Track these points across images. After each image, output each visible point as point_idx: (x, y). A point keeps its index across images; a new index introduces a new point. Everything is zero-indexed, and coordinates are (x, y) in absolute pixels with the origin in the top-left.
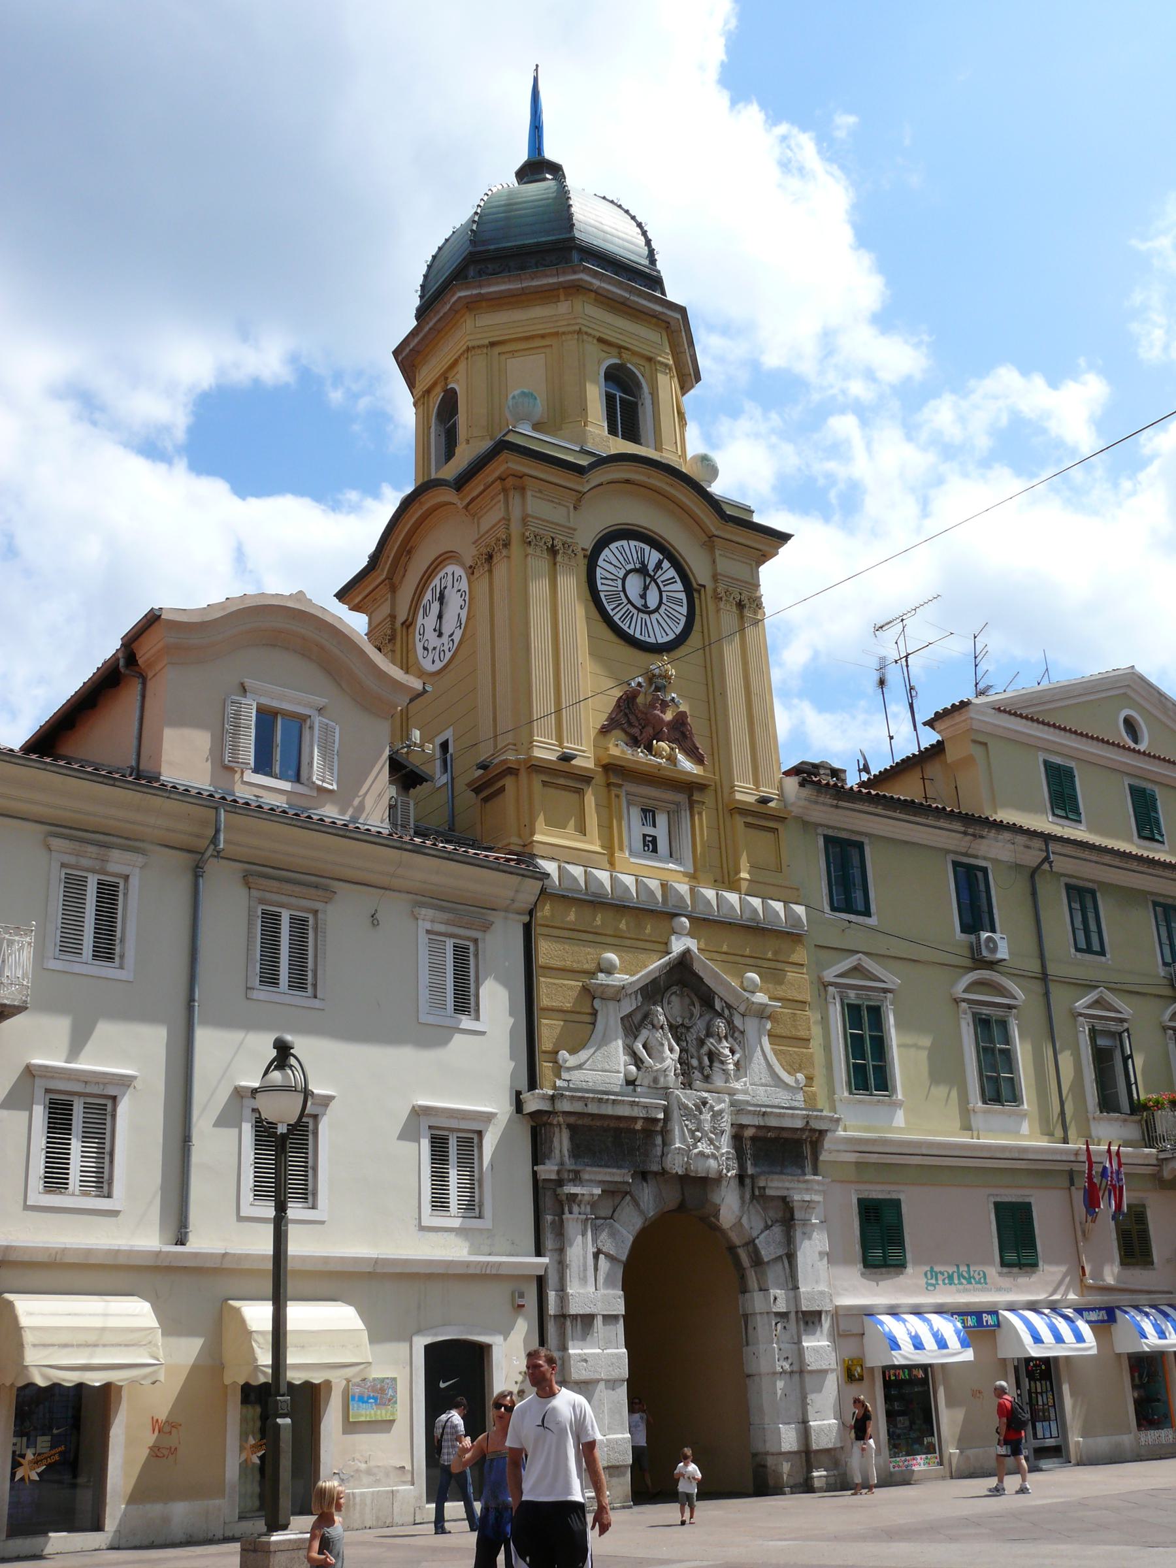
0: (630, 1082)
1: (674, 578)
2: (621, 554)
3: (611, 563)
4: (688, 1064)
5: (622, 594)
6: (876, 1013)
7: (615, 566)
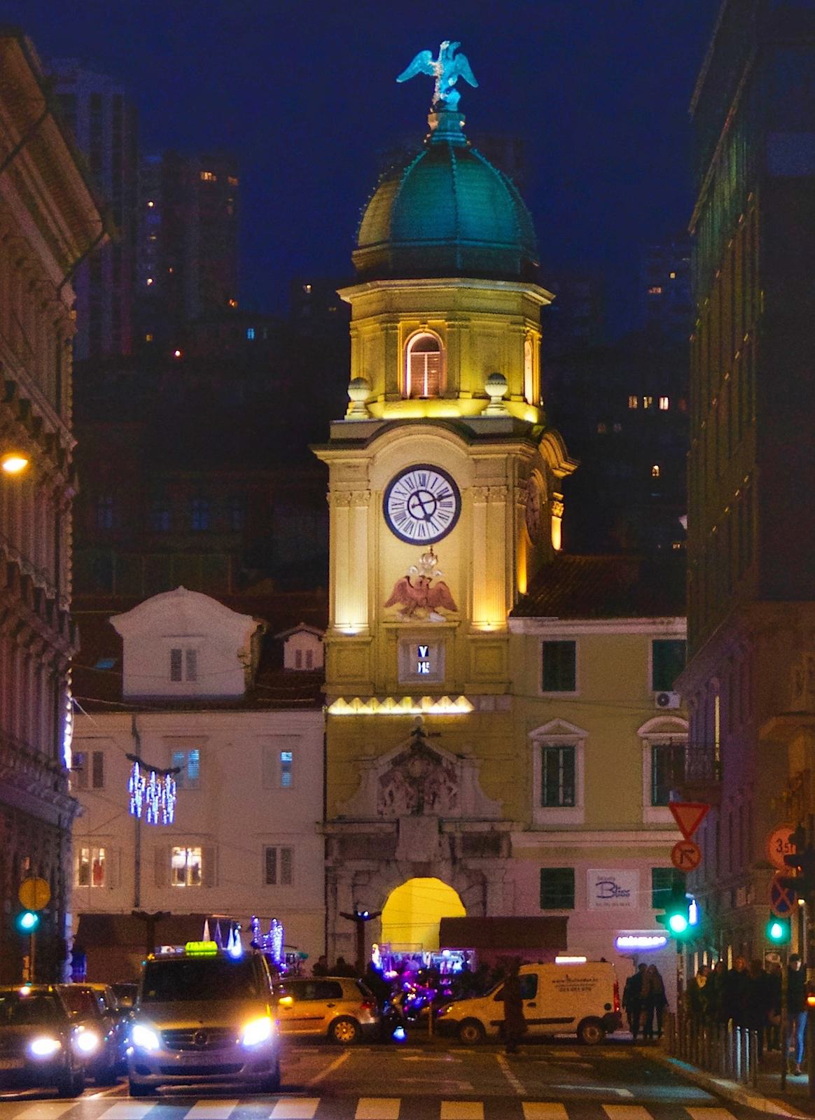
0: (381, 813)
1: (447, 488)
2: (408, 483)
3: (400, 492)
4: (423, 798)
5: (407, 512)
6: (570, 752)
7: (403, 494)
